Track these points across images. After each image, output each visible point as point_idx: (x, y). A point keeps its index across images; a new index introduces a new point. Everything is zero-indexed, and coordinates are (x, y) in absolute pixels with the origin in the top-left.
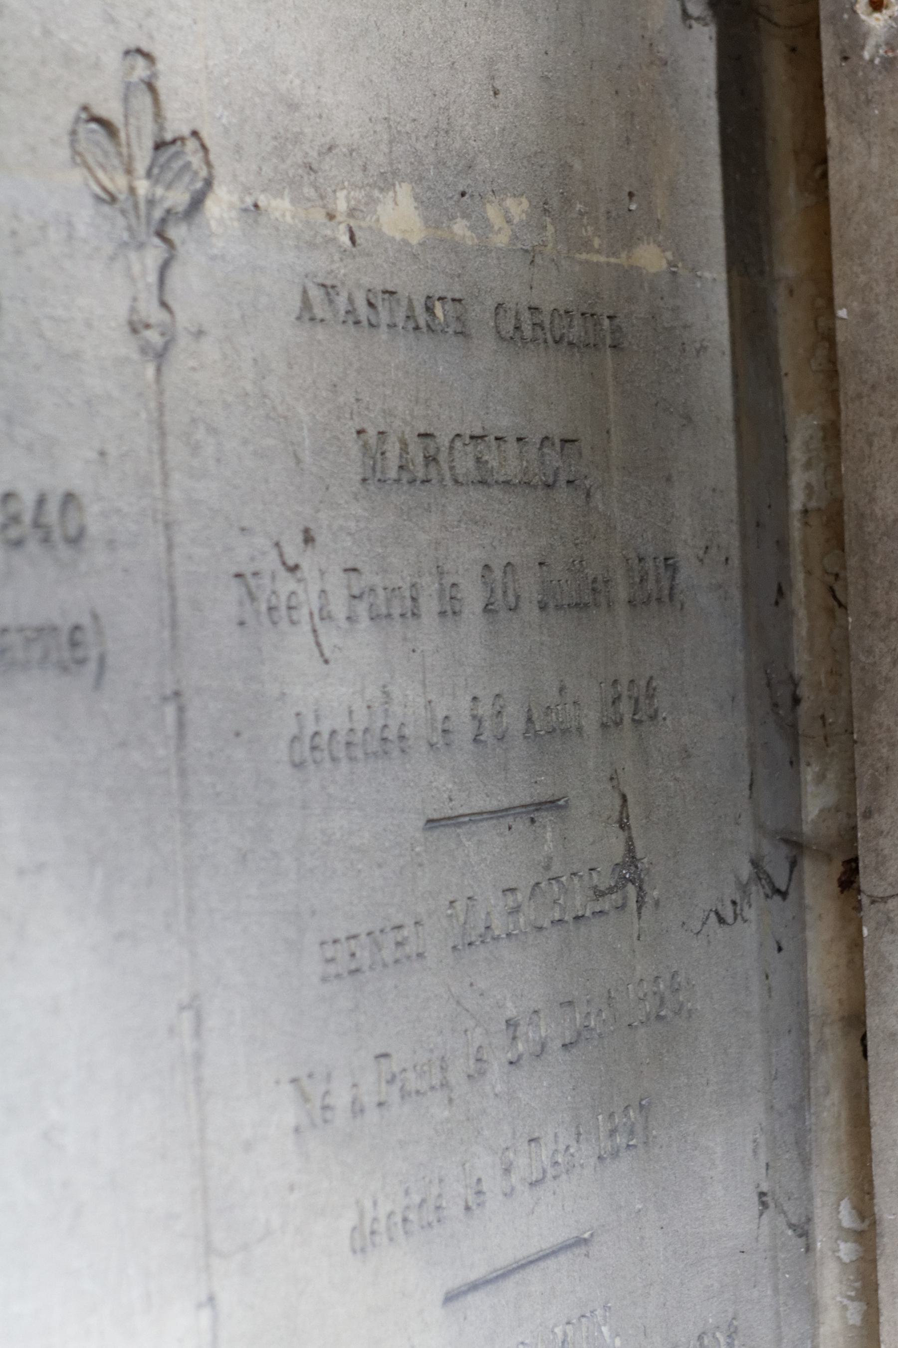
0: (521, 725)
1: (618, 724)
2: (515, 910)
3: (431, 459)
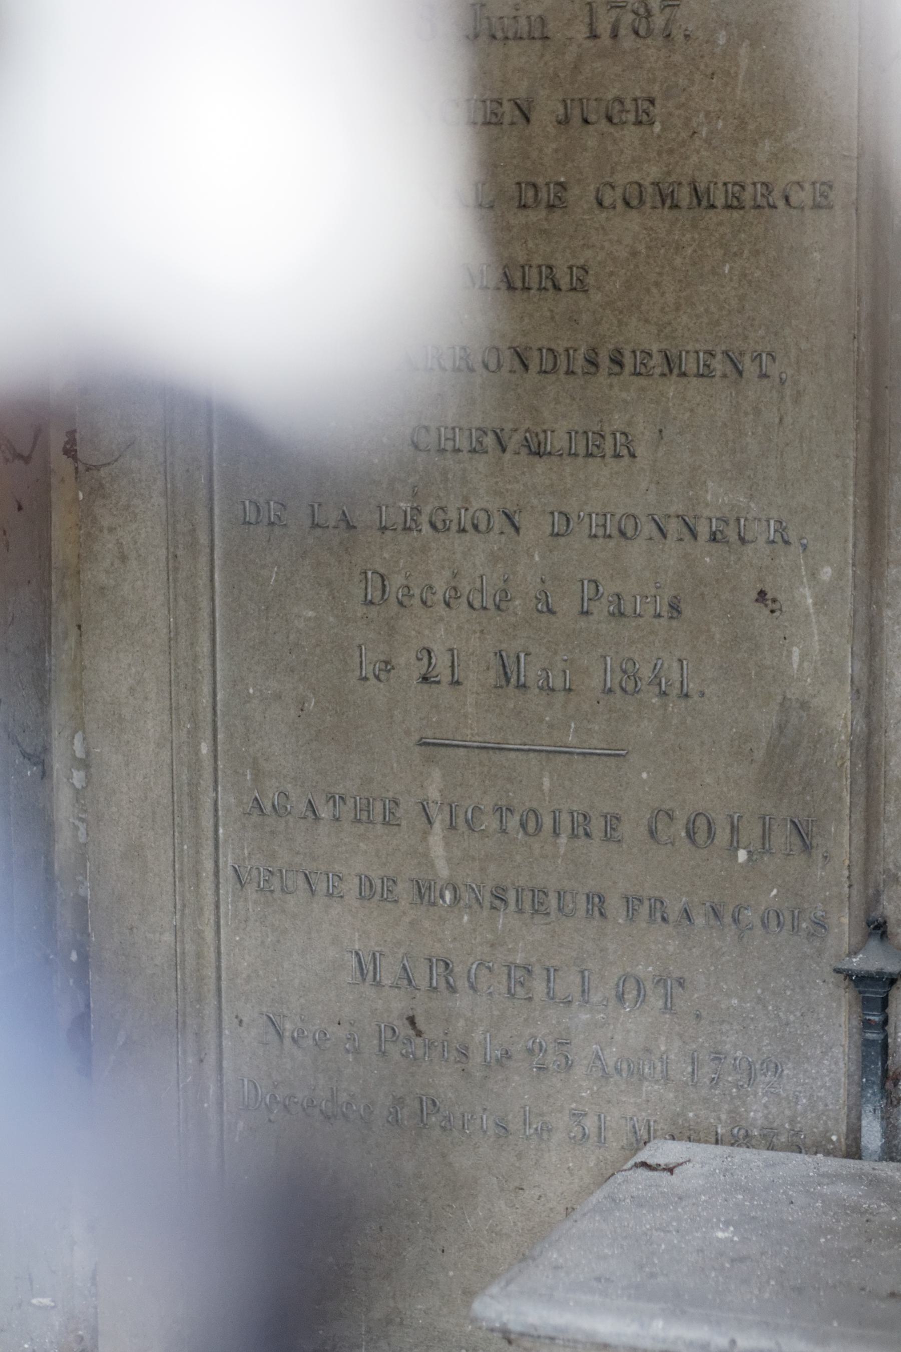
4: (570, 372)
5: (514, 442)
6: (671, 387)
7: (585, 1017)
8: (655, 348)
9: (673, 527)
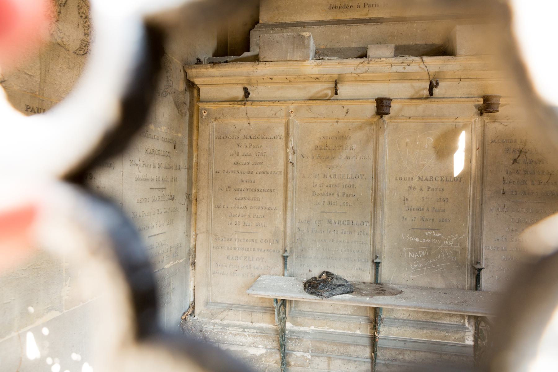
0: (162, 180)
1: (173, 181)
2: (159, 198)
3: (153, 152)
4: (253, 191)
5: (246, 199)
6: (264, 193)
7: (252, 262)
8: (262, 189)
9: (264, 208)
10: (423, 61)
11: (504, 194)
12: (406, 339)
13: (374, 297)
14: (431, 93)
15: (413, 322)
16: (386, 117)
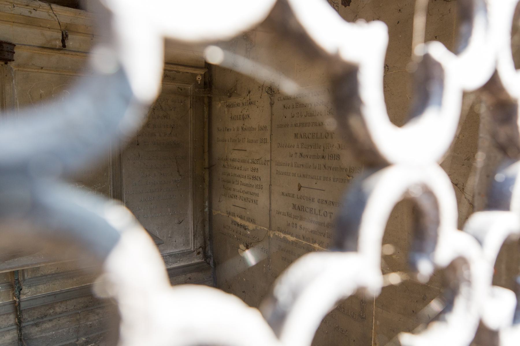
10: (51, 8)
11: (138, 145)
12: (56, 292)
13: (6, 262)
14: (64, 46)
15: (62, 274)
16: (12, 65)
